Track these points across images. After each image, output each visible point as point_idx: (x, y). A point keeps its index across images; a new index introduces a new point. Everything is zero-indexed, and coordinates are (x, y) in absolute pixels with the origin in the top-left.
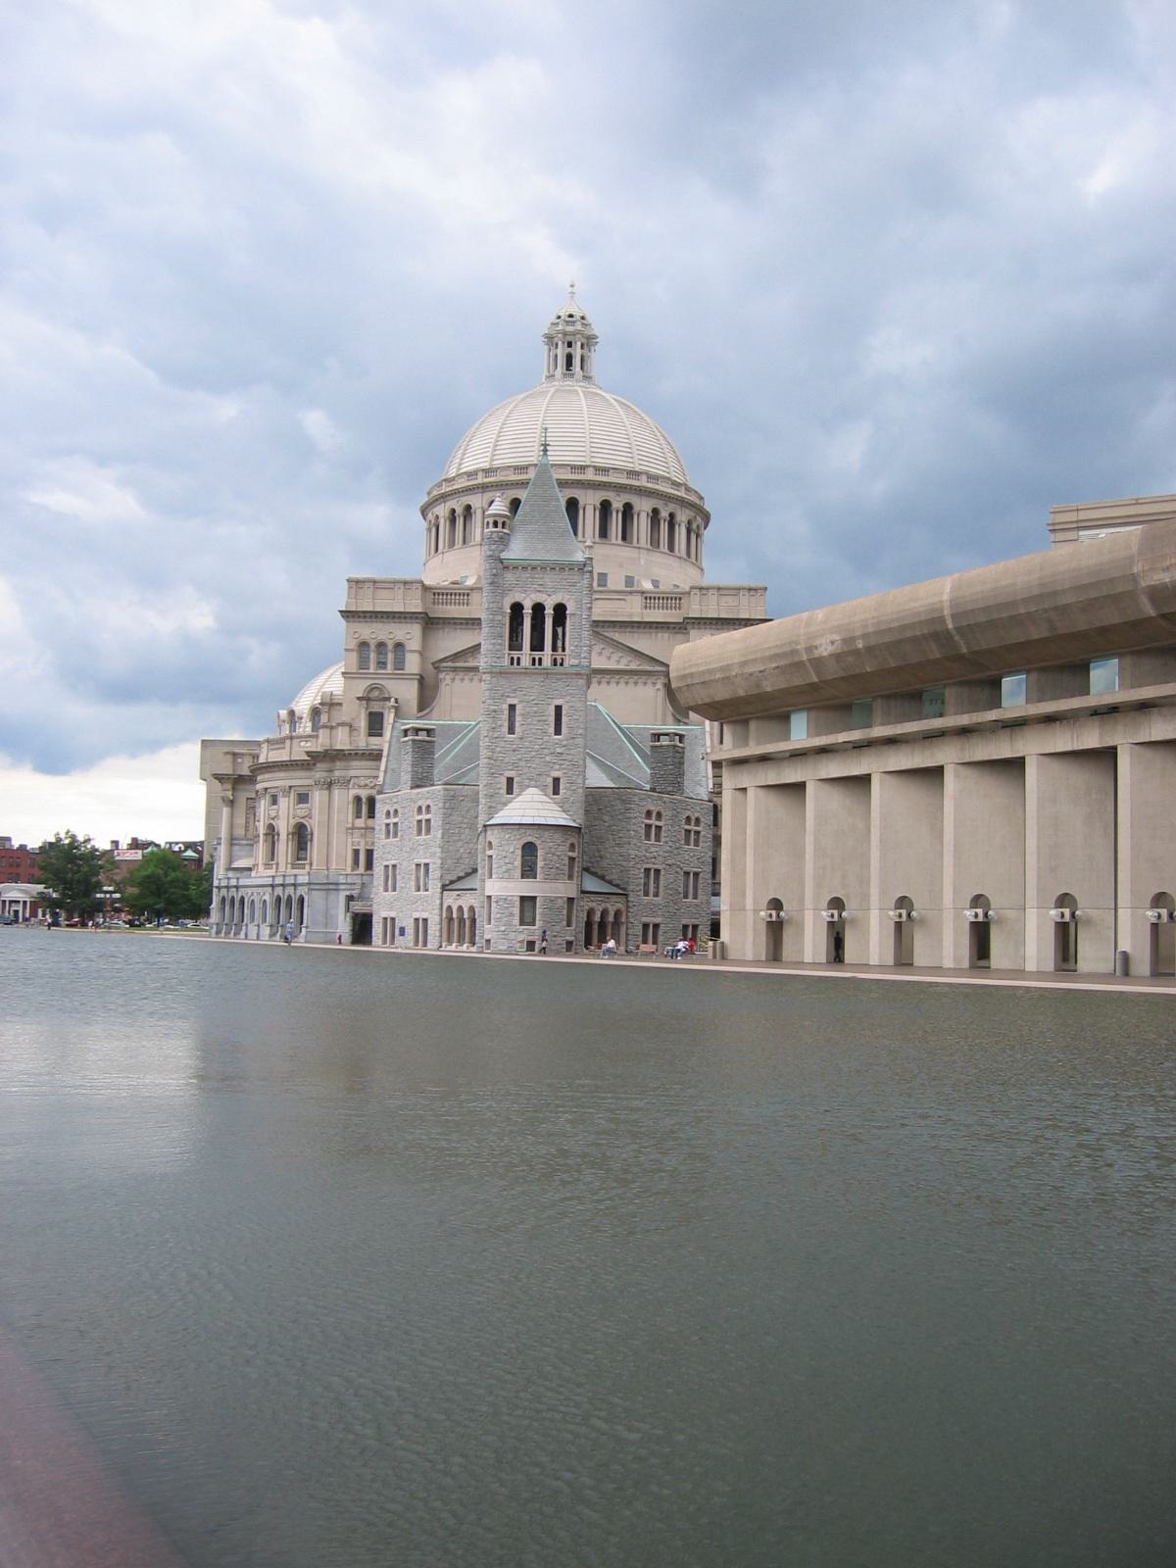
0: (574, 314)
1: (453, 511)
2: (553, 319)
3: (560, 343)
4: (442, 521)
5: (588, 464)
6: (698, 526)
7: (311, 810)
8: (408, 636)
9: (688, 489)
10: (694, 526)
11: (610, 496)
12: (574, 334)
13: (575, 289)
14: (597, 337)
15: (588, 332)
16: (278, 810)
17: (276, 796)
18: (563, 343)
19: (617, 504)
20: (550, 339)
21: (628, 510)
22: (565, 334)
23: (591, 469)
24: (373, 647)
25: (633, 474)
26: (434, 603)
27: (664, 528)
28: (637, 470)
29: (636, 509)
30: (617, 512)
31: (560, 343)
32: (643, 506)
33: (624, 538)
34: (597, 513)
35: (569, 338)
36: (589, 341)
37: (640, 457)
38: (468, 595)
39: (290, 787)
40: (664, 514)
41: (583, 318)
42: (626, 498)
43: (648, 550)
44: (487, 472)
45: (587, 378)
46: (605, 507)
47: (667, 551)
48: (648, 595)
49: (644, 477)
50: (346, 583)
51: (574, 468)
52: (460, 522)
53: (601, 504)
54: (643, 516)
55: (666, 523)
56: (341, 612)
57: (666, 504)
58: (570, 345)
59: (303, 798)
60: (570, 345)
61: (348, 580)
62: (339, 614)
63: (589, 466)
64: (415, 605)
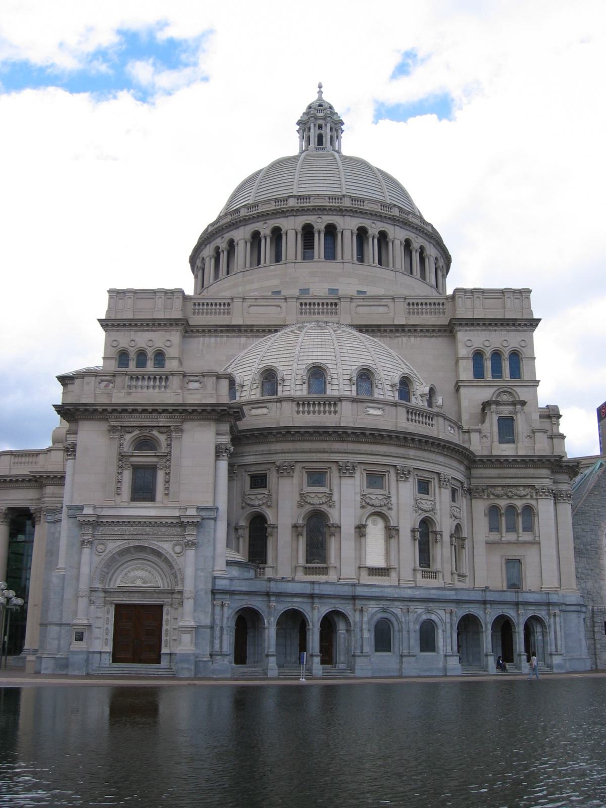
1: (217, 248)
3: (312, 125)
4: (207, 260)
6: (442, 266)
8: (168, 344)
12: (325, 118)
13: (322, 89)
18: (315, 125)
19: (374, 228)
22: (316, 118)
25: (383, 205)
26: (194, 313)
29: (391, 236)
31: (312, 125)
32: (397, 235)
33: (380, 263)
35: (321, 122)
36: (337, 125)
38: (229, 304)
40: (416, 245)
42: (381, 226)
46: (362, 234)
48: (411, 301)
50: (107, 296)
52: (223, 258)
53: (358, 229)
55: (418, 254)
56: (99, 320)
57: (416, 237)
58: (320, 127)
60: (320, 127)
61: (111, 292)
62: (98, 324)
63: (344, 196)
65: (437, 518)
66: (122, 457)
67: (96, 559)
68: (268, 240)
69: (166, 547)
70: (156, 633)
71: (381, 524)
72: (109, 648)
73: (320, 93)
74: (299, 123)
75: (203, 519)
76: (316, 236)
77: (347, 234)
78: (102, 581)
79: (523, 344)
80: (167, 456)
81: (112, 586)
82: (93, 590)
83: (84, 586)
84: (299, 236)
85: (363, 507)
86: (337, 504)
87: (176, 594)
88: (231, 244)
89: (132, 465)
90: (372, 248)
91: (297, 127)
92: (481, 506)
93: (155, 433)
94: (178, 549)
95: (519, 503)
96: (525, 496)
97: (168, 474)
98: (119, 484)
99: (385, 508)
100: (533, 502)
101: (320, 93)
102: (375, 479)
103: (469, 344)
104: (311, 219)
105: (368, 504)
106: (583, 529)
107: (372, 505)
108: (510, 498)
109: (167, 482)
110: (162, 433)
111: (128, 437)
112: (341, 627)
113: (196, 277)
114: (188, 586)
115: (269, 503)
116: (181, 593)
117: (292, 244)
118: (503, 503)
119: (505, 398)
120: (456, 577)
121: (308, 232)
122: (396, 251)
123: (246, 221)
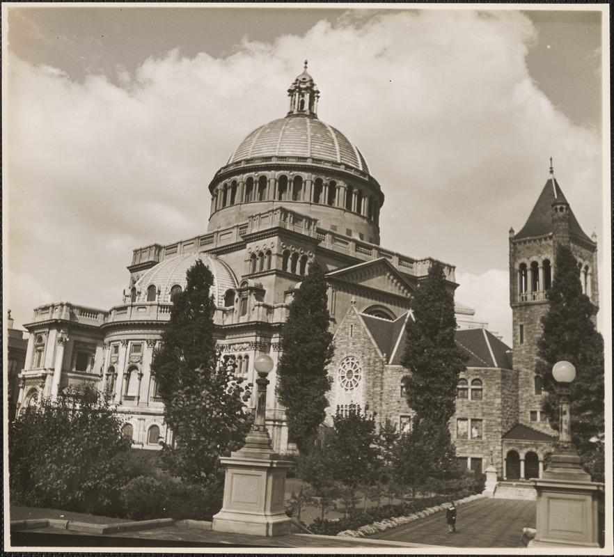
1: (225, 185)
2: (294, 82)
4: (219, 191)
7: (141, 357)
9: (371, 178)
12: (306, 89)
13: (307, 65)
14: (318, 92)
15: (315, 89)
16: (118, 357)
17: (118, 347)
19: (325, 180)
20: (291, 92)
21: (333, 188)
23: (311, 160)
28: (339, 161)
34: (313, 186)
36: (314, 94)
39: (128, 340)
43: (345, 211)
44: (248, 161)
45: (313, 116)
46: (318, 185)
49: (343, 167)
52: (229, 192)
58: (303, 96)
59: (137, 348)
73: (306, 67)
74: (289, 91)
76: (288, 184)
77: (308, 183)
84: (277, 183)
88: (235, 184)
91: (288, 93)
101: (306, 67)
113: (213, 199)
121: (283, 181)
123: (244, 171)
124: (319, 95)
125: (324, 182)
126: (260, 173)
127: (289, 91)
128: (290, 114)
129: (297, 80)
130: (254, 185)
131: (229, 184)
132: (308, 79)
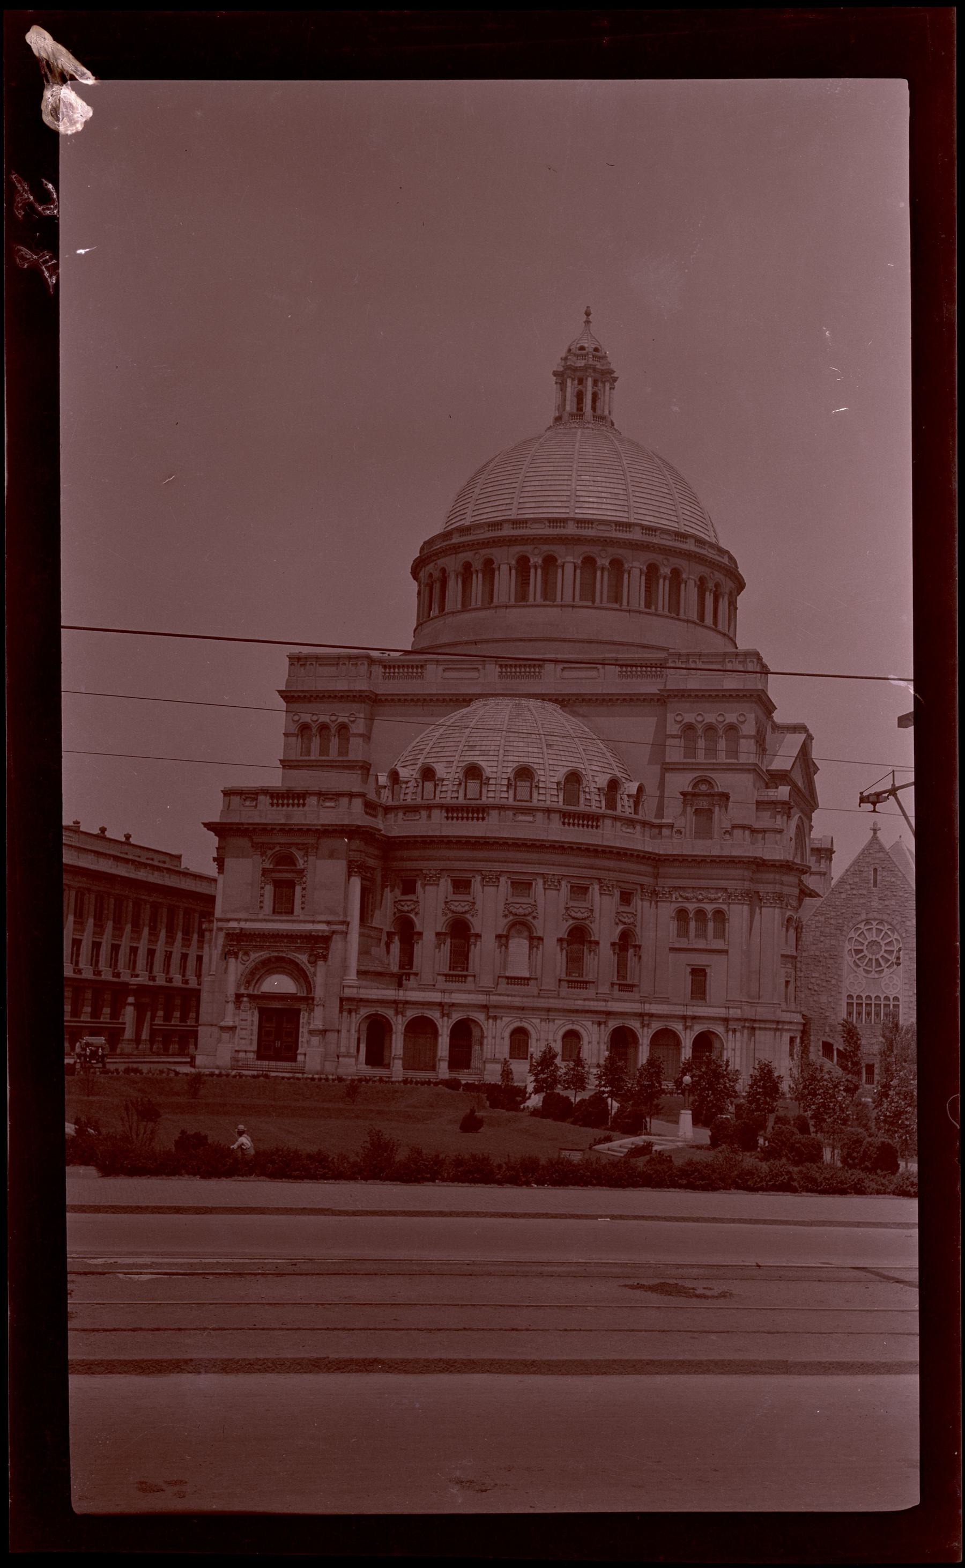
0: (586, 345)
2: (563, 355)
5: (572, 515)
10: (711, 585)
11: (593, 550)
12: (585, 368)
14: (613, 372)
20: (561, 377)
22: (575, 369)
24: (314, 730)
27: (663, 588)
30: (603, 569)
35: (579, 374)
36: (606, 376)
37: (638, 505)
40: (665, 571)
41: (596, 350)
47: (666, 612)
49: (638, 529)
51: (554, 522)
54: (636, 572)
55: (667, 582)
56: (279, 691)
57: (666, 559)
58: (581, 381)
64: (361, 685)
65: (594, 927)
66: (265, 872)
67: (241, 967)
68: (480, 575)
69: (302, 958)
70: (294, 1034)
71: (526, 934)
72: (254, 1047)
73: (588, 322)
74: (555, 374)
75: (334, 932)
76: (532, 571)
78: (247, 988)
79: (742, 719)
80: (302, 871)
81: (256, 993)
82: (238, 997)
83: (231, 991)
84: (513, 572)
85: (506, 916)
86: (480, 912)
87: (308, 1000)
89: (273, 880)
90: (602, 582)
92: (667, 910)
93: (293, 850)
94: (313, 959)
95: (709, 908)
96: (715, 899)
97: (304, 889)
98: (262, 898)
99: (529, 918)
100: (725, 907)
101: (588, 322)
102: (522, 886)
103: (679, 718)
104: (527, 549)
105: (511, 912)
106: (821, 932)
107: (516, 915)
108: (699, 901)
109: (303, 896)
110: (299, 849)
111: (270, 853)
112: (476, 1032)
114: (319, 993)
115: (417, 910)
116: (313, 999)
117: (505, 581)
118: (691, 907)
119: (704, 788)
120: (616, 987)
122: (635, 584)
123: (456, 549)
124: (615, 375)
125: (600, 562)
126: (483, 552)
127: (555, 374)
128: (558, 419)
129: (569, 350)
130: (474, 576)
131: (437, 574)
132: (589, 345)
